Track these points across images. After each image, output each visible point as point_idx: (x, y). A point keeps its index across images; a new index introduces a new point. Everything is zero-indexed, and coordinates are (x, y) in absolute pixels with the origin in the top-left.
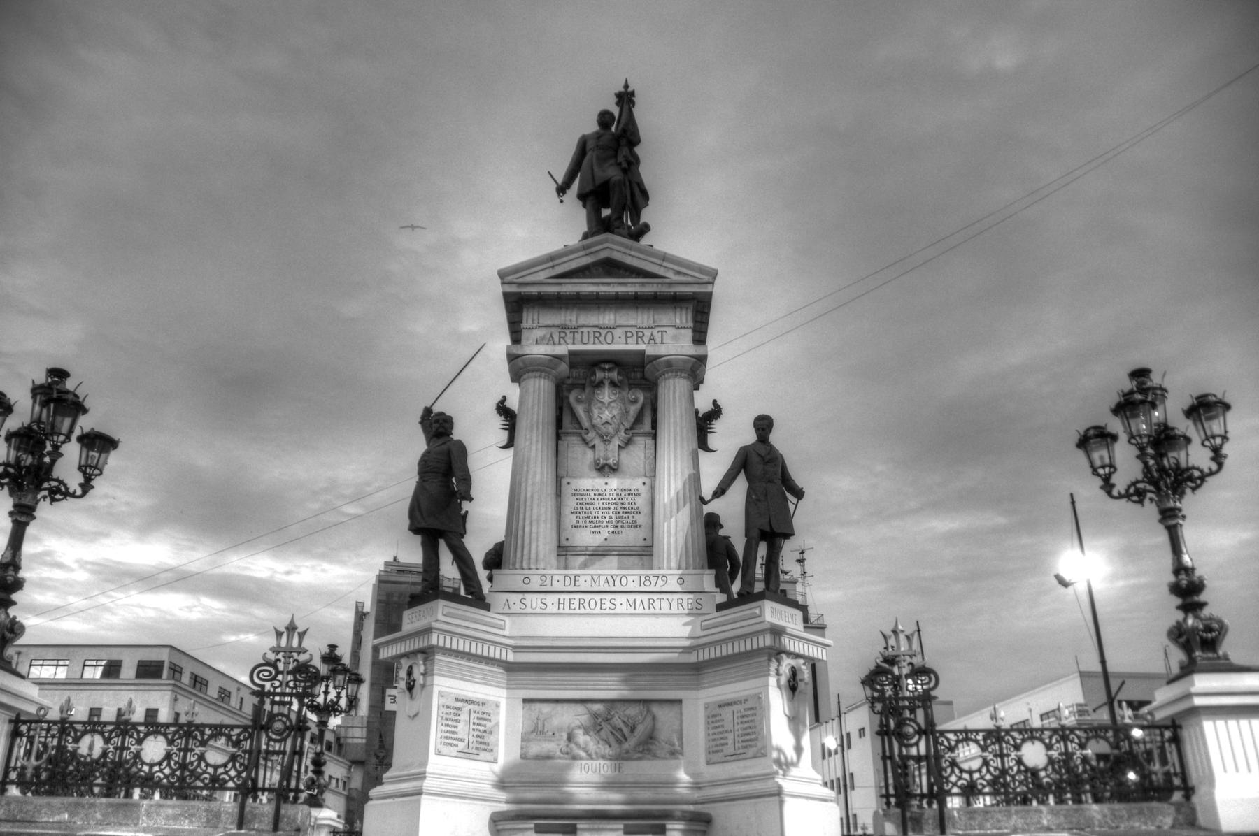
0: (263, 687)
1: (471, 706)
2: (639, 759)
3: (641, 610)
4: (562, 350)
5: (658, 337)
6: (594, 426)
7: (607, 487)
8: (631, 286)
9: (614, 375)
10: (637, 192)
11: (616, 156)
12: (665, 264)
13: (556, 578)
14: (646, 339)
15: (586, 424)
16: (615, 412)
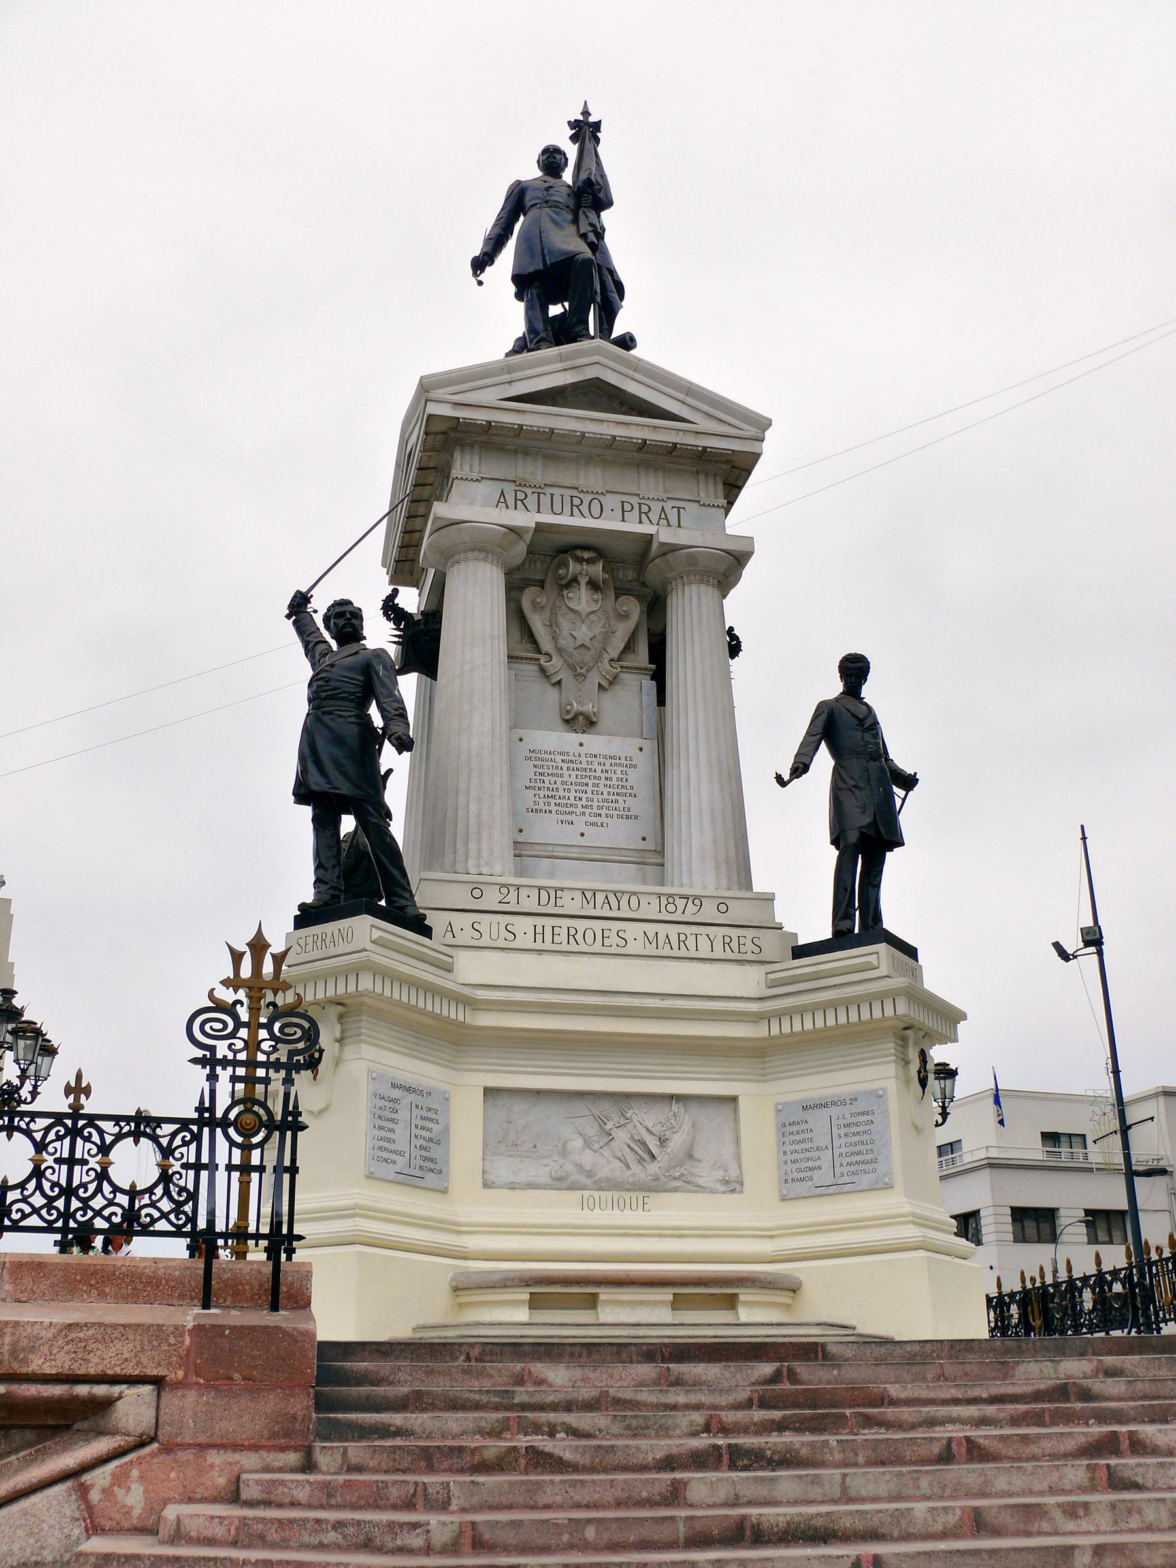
0: (212, 1049)
1: (412, 1097)
2: (675, 1190)
3: (667, 951)
4: (525, 519)
5: (673, 516)
6: (559, 650)
7: (583, 750)
8: (636, 429)
9: (597, 570)
10: (611, 284)
11: (576, 221)
12: (689, 400)
13: (523, 892)
14: (654, 516)
15: (546, 644)
16: (597, 630)
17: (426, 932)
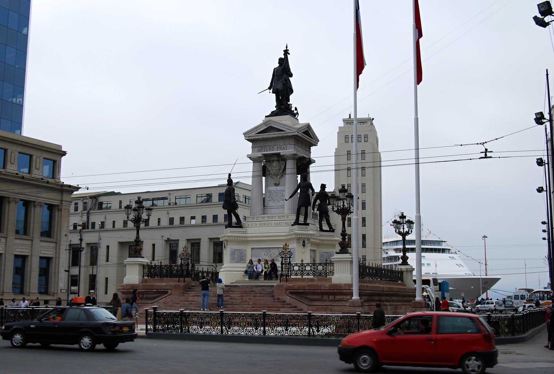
10: (288, 90)
17: (242, 227)
